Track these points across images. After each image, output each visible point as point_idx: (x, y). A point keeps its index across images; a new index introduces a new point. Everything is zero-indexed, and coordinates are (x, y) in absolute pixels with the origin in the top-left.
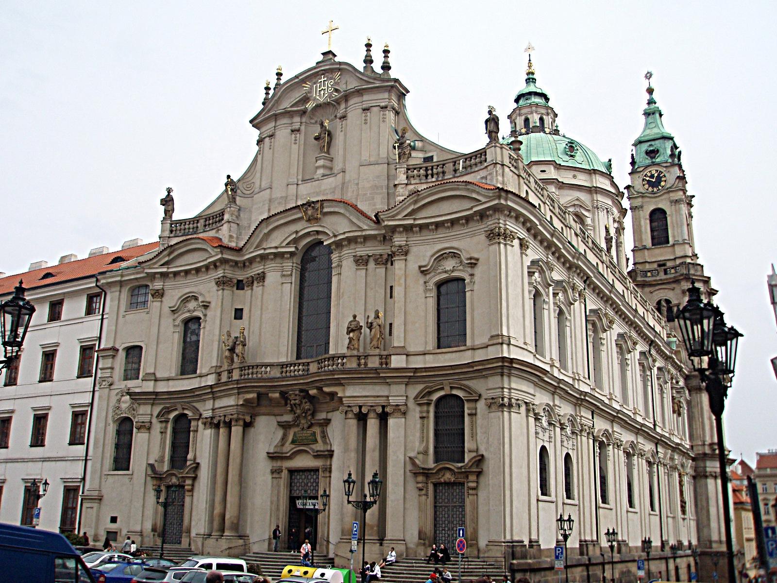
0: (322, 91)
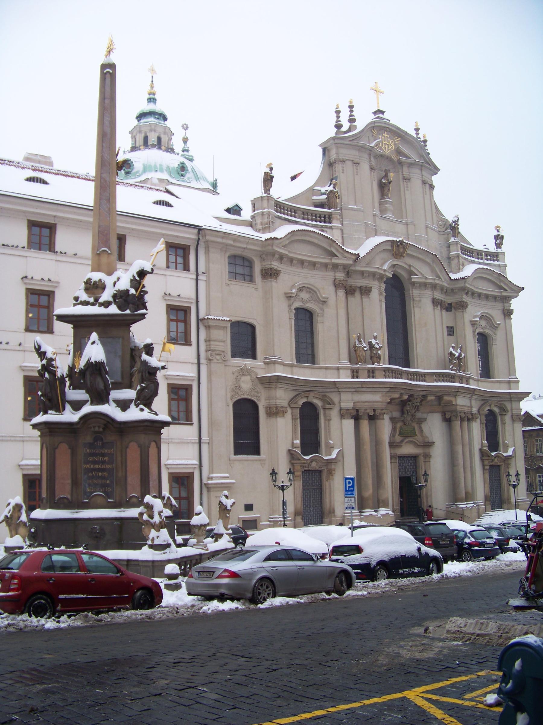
0: (387, 145)
